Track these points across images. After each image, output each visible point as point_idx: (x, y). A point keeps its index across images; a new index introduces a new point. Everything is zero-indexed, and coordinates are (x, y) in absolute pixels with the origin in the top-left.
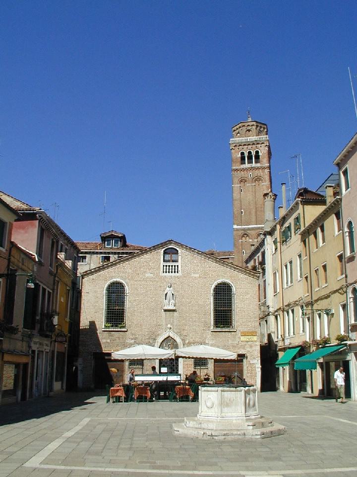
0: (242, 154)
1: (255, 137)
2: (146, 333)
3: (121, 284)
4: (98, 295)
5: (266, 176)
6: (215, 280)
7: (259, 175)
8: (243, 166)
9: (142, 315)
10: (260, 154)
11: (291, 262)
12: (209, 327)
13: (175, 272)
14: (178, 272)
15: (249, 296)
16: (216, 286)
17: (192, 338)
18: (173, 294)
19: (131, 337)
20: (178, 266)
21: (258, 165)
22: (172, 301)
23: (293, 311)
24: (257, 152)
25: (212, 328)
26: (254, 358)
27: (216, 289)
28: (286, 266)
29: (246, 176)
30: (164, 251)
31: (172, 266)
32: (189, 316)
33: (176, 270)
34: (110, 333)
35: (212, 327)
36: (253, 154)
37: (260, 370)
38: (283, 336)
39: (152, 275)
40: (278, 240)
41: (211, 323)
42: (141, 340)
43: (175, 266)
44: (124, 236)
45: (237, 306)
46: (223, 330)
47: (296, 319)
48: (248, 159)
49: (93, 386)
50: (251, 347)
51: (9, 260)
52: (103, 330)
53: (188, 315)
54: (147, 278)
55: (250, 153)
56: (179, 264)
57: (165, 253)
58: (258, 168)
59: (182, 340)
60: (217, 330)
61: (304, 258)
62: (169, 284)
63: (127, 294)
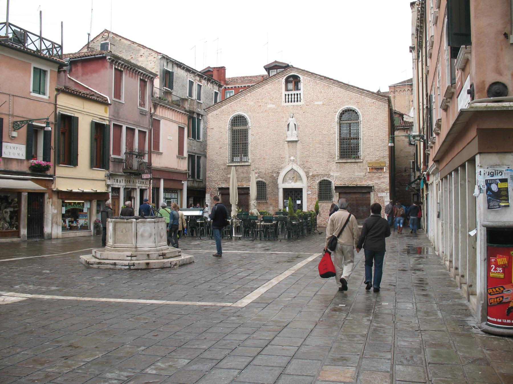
2: (270, 167)
3: (243, 117)
4: (223, 130)
12: (334, 158)
14: (300, 101)
17: (316, 170)
18: (295, 125)
20: (300, 94)
22: (294, 132)
25: (337, 159)
26: (383, 192)
33: (299, 99)
35: (337, 157)
39: (273, 106)
41: (335, 154)
42: (265, 174)
43: (297, 94)
45: (364, 134)
46: (349, 161)
51: (56, 105)
52: (227, 165)
53: (311, 146)
54: (270, 108)
56: (301, 92)
57: (287, 81)
60: (342, 161)
62: (291, 114)
63: (250, 128)
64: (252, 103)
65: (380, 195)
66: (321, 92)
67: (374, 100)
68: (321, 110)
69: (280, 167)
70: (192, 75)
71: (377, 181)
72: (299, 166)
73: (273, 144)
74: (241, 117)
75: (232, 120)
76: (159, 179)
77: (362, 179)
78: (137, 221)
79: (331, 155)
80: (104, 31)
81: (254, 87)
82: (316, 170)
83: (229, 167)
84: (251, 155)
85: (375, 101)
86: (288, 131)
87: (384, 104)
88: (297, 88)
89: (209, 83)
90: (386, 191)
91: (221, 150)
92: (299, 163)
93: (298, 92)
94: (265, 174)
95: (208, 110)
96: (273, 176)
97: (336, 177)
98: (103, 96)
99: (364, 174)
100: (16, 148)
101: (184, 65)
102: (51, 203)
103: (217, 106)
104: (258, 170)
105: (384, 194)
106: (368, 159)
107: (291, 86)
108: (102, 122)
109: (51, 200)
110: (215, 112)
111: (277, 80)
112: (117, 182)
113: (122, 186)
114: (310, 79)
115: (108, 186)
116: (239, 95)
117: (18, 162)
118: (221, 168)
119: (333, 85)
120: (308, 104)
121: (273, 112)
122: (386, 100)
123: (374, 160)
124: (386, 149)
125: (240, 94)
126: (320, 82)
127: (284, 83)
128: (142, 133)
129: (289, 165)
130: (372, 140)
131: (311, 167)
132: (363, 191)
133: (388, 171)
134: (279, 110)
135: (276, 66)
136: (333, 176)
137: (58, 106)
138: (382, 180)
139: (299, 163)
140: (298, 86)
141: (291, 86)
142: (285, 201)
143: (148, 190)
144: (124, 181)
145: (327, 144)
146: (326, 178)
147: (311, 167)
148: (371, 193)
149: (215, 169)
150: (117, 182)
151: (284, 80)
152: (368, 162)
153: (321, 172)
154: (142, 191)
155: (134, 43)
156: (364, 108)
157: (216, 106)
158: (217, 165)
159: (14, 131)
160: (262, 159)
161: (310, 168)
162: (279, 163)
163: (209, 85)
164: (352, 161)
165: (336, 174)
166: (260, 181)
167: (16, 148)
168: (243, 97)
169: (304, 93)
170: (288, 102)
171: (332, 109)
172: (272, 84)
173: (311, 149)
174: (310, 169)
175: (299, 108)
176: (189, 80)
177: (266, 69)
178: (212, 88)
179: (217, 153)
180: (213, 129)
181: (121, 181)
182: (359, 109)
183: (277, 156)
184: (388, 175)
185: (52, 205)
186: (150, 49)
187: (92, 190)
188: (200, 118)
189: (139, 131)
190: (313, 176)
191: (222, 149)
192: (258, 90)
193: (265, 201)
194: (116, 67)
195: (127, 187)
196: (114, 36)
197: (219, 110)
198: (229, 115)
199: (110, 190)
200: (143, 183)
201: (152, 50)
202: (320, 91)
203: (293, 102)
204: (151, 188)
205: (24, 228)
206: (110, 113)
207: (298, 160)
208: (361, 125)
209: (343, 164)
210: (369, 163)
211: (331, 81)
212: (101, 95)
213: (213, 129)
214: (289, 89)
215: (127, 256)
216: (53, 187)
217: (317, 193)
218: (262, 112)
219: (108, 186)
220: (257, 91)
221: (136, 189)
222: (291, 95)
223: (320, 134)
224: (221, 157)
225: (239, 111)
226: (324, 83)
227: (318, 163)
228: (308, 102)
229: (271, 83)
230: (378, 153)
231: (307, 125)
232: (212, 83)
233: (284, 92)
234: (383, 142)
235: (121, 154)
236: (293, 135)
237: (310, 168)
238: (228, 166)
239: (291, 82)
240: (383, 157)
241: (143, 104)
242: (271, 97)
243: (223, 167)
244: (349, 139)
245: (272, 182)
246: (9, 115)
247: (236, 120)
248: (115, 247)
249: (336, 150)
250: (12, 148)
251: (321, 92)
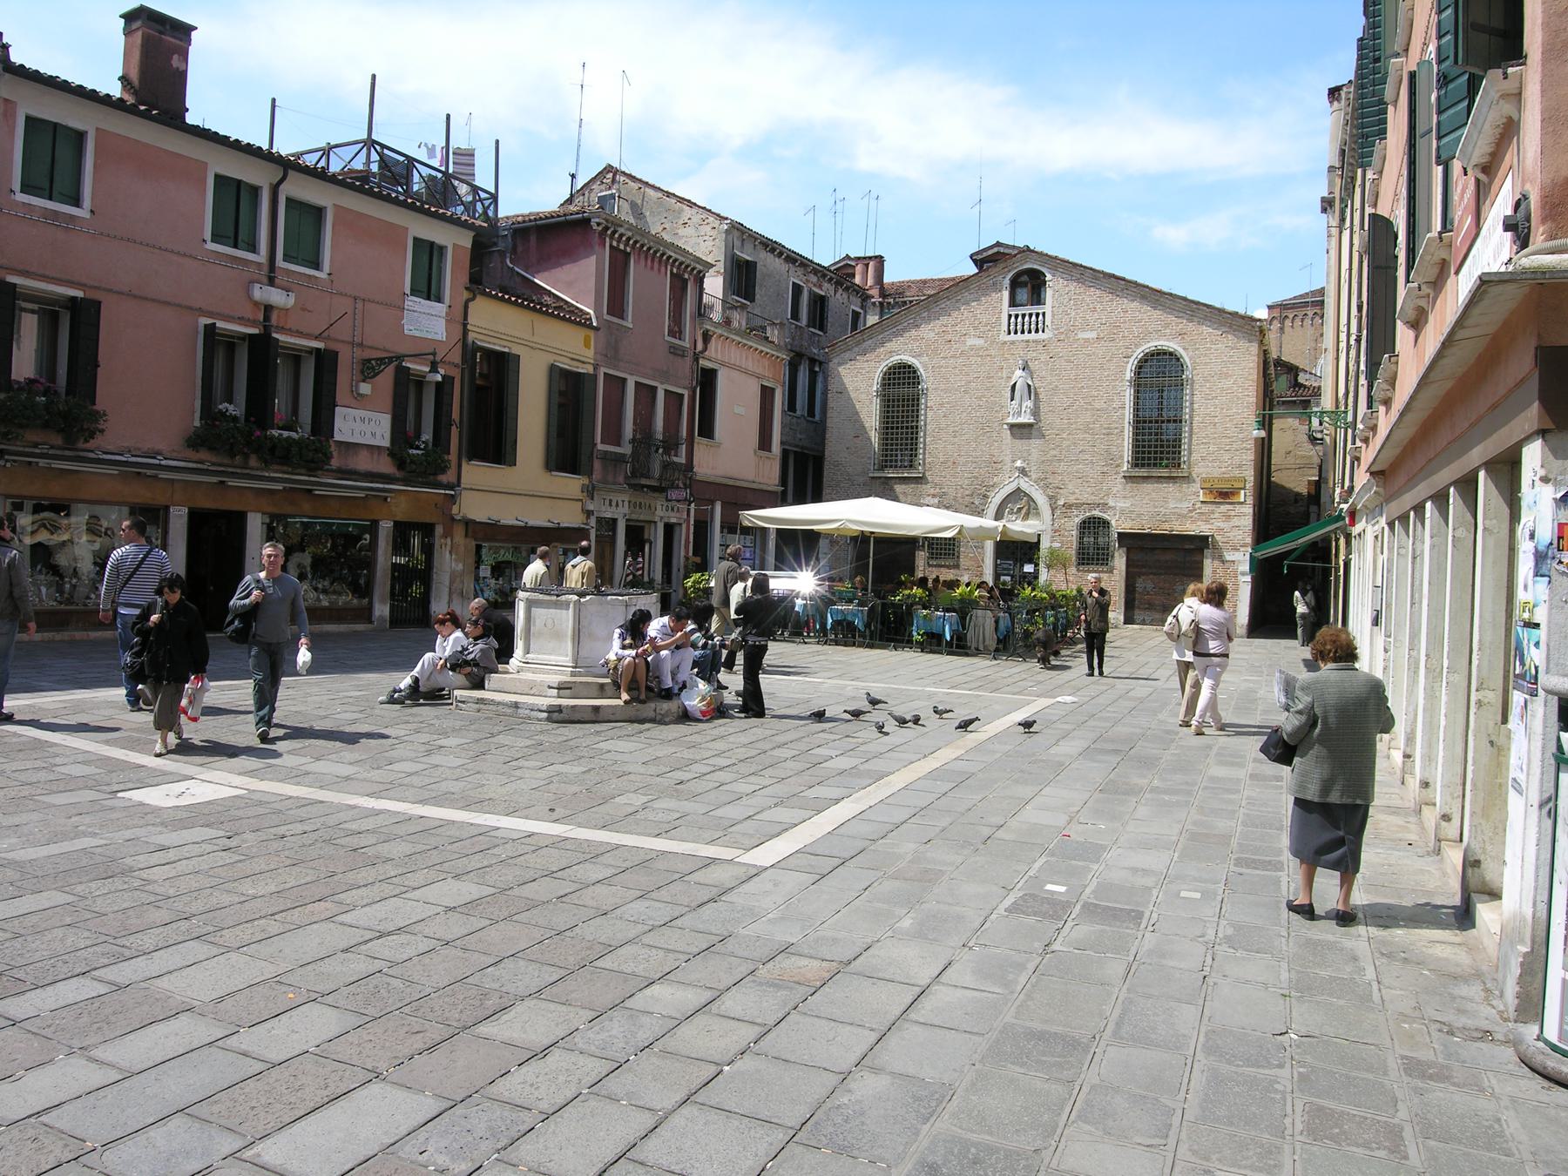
3: (910, 366)
4: (863, 396)
6: (1137, 346)
12: (1118, 466)
14: (1043, 331)
15: (1229, 383)
17: (1074, 493)
18: (1029, 386)
19: (932, 491)
20: (1044, 314)
22: (1029, 404)
25: (1125, 468)
32: (1069, 440)
34: (887, 484)
39: (980, 342)
41: (1122, 457)
42: (955, 499)
43: (1037, 315)
50: (1228, 517)
51: (465, 325)
52: (871, 475)
53: (1064, 436)
56: (1047, 308)
57: (1015, 284)
59: (1051, 498)
64: (932, 335)
70: (800, 271)
71: (1222, 525)
74: (904, 367)
75: (885, 374)
76: (712, 502)
77: (1184, 516)
78: (582, 600)
80: (605, 169)
82: (1074, 493)
83: (874, 481)
88: (1037, 298)
89: (840, 291)
90: (1242, 549)
92: (1034, 477)
94: (955, 499)
97: (1122, 512)
98: (581, 310)
100: (367, 422)
101: (783, 247)
102: (448, 548)
106: (1201, 470)
107: (1023, 294)
108: (578, 367)
109: (449, 540)
112: (610, 505)
113: (622, 515)
115: (589, 513)
117: (372, 454)
123: (1216, 473)
128: (674, 399)
132: (1187, 547)
133: (1250, 500)
134: (993, 352)
135: (998, 253)
136: (1113, 508)
137: (469, 327)
138: (1235, 522)
139: (1034, 477)
140: (1039, 295)
141: (1023, 294)
142: (999, 561)
143: (684, 526)
144: (626, 504)
145: (1104, 431)
146: (1096, 513)
149: (842, 485)
150: (610, 505)
153: (1086, 497)
154: (669, 529)
155: (669, 194)
159: (364, 381)
162: (987, 475)
163: (838, 295)
165: (1121, 504)
167: (367, 422)
173: (1066, 443)
174: (1061, 491)
176: (794, 283)
177: (975, 261)
178: (845, 301)
181: (620, 504)
184: (1248, 510)
185: (450, 552)
186: (704, 208)
187: (549, 521)
188: (817, 369)
189: (666, 390)
190: (1068, 506)
194: (615, 244)
195: (634, 517)
196: (627, 181)
199: (593, 522)
200: (673, 509)
201: (710, 211)
204: (692, 522)
205: (383, 601)
206: (595, 348)
210: (1204, 481)
212: (577, 308)
214: (1018, 302)
215: (550, 687)
216: (455, 510)
217: (1074, 547)
219: (589, 513)
220: (943, 306)
221: (655, 522)
222: (1024, 316)
223: (1087, 409)
230: (1226, 457)
232: (847, 289)
235: (622, 442)
238: (873, 478)
239: (1024, 285)
240: (1240, 466)
241: (676, 331)
242: (977, 322)
243: (861, 480)
244: (1157, 422)
246: (353, 344)
248: (528, 663)
250: (358, 419)
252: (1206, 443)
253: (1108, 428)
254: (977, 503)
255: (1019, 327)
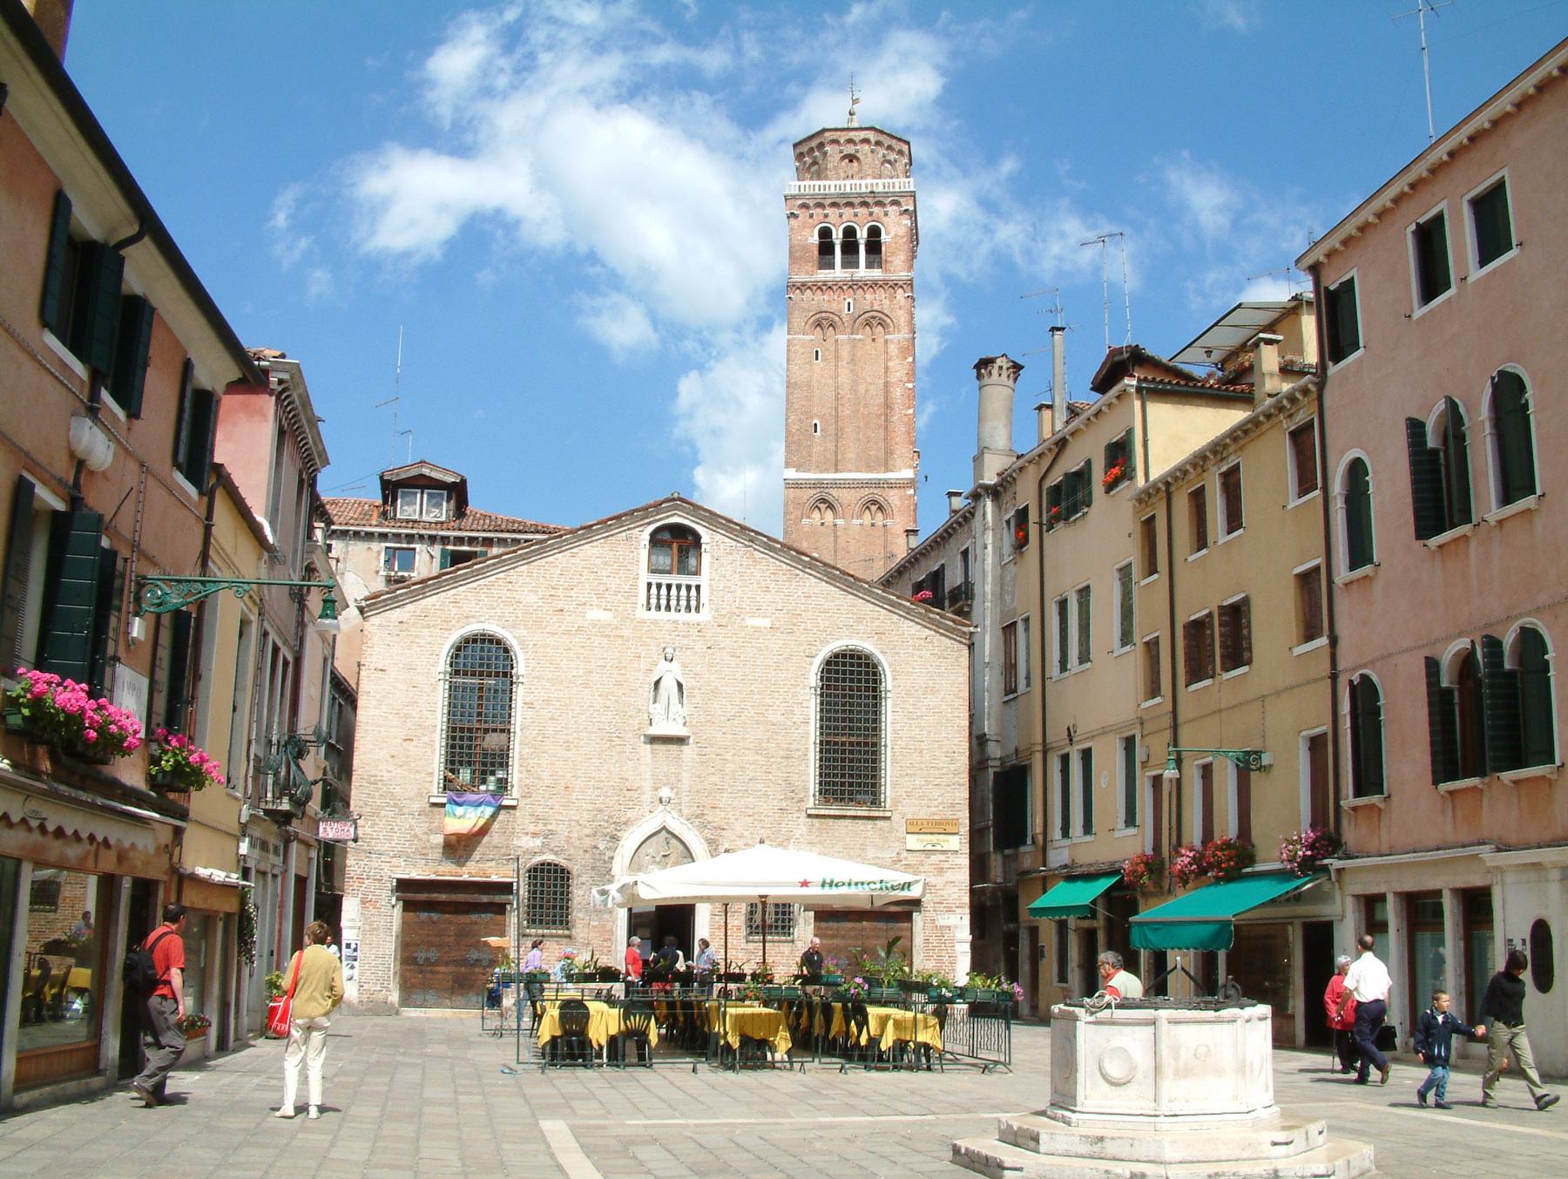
0: (825, 234)
1: (869, 181)
5: (902, 312)
6: (824, 642)
7: (876, 308)
8: (824, 275)
9: (569, 754)
10: (884, 237)
11: (1084, 593)
12: (801, 800)
13: (668, 608)
14: (698, 609)
16: (828, 663)
18: (680, 686)
19: (532, 828)
20: (698, 588)
21: (876, 273)
22: (675, 706)
23: (1087, 755)
24: (874, 232)
25: (811, 804)
26: (950, 911)
27: (829, 671)
28: (1063, 604)
29: (834, 307)
30: (653, 535)
31: (679, 587)
33: (693, 603)
35: (812, 799)
36: (862, 235)
37: (967, 948)
38: (1040, 838)
39: (608, 616)
40: (1033, 516)
41: (806, 789)
43: (689, 588)
44: (463, 482)
47: (1100, 781)
48: (844, 252)
49: (394, 997)
50: (941, 871)
52: (433, 800)
53: (728, 756)
55: (850, 233)
56: (704, 580)
57: (656, 541)
58: (874, 285)
61: (1140, 582)
64: (533, 598)
65: (943, 920)
66: (767, 590)
67: (928, 632)
68: (766, 647)
69: (623, 819)
72: (688, 820)
73: (599, 741)
79: (793, 791)
81: (543, 548)
84: (521, 772)
85: (932, 633)
86: (655, 702)
87: (956, 645)
90: (958, 911)
91: (410, 746)
92: (686, 811)
93: (693, 581)
95: (368, 606)
96: (595, 847)
99: (894, 854)
103: (406, 593)
104: (545, 825)
105: (953, 917)
107: (665, 560)
110: (396, 615)
111: (624, 534)
114: (734, 543)
116: (488, 566)
118: (405, 811)
119: (807, 570)
120: (724, 621)
121: (606, 636)
122: (964, 633)
124: (962, 781)
125: (494, 564)
126: (763, 555)
127: (648, 546)
129: (652, 815)
130: (921, 752)
131: (727, 823)
134: (626, 633)
138: (949, 876)
139: (686, 811)
145: (782, 753)
147: (727, 823)
148: (914, 914)
149: (383, 813)
151: (648, 538)
152: (907, 817)
156: (899, 653)
157: (401, 595)
158: (393, 796)
160: (561, 788)
161: (724, 829)
164: (859, 813)
166: (549, 864)
168: (502, 575)
169: (710, 586)
170: (658, 607)
171: (801, 645)
172: (606, 543)
173: (729, 767)
174: (724, 833)
175: (694, 632)
179: (393, 757)
180: (382, 670)
182: (882, 652)
183: (612, 783)
191: (415, 743)
192: (556, 556)
193: (566, 932)
197: (410, 607)
198: (446, 629)
202: (763, 584)
203: (663, 608)
207: (685, 800)
208: (889, 701)
209: (830, 821)
211: (804, 558)
213: (382, 670)
218: (567, 633)
220: (551, 559)
222: (669, 587)
224: (410, 771)
225: (482, 619)
226: (778, 563)
227: (751, 812)
228: (725, 616)
229: (602, 541)
230: (936, 793)
231: (716, 687)
233: (645, 577)
234: (952, 761)
236: (671, 716)
237: (724, 829)
240: (953, 805)
242: (602, 588)
245: (593, 868)
247: (859, 665)
249: (808, 775)
251: (767, 590)
252: (911, 775)
253: (788, 750)
254: (601, 846)
255: (663, 602)
